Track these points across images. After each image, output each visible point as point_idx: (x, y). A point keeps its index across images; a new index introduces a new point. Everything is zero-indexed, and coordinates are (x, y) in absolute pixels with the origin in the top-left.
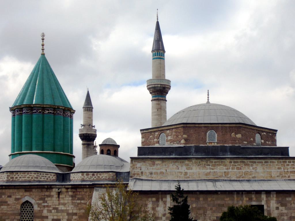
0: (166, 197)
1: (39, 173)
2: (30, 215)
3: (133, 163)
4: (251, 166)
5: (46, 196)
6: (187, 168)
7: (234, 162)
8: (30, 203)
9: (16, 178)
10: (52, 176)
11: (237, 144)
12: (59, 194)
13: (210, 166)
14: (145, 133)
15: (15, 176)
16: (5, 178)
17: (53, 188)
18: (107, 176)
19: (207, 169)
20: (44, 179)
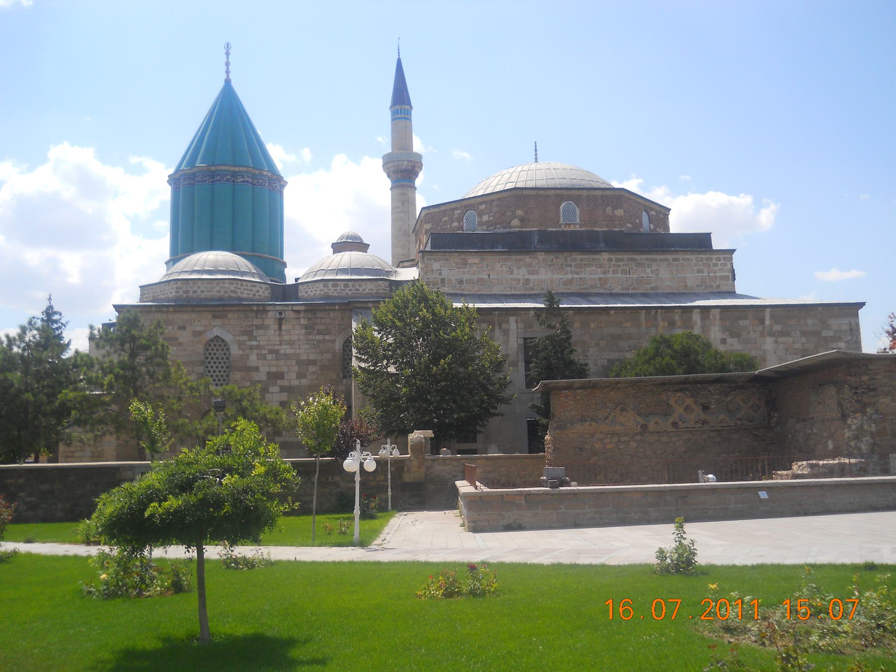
0: (507, 322)
1: (240, 283)
3: (426, 262)
4: (648, 268)
5: (254, 327)
6: (528, 271)
7: (618, 260)
8: (223, 341)
9: (195, 292)
10: (263, 290)
11: (616, 227)
12: (280, 321)
14: (433, 213)
17: (269, 311)
18: (374, 288)
19: (567, 274)
20: (247, 294)
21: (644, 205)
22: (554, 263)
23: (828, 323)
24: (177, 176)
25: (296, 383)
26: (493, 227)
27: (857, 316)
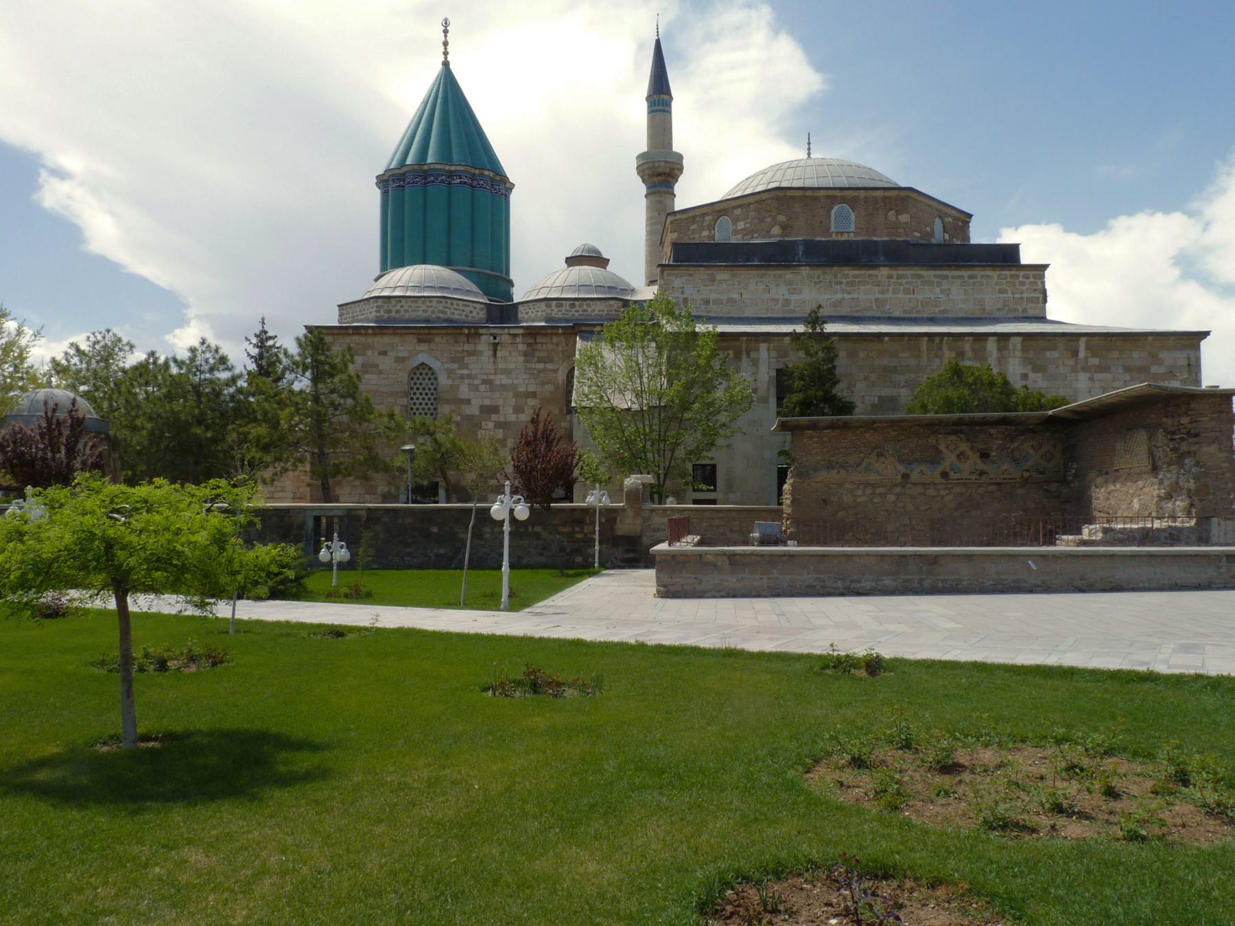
0: (758, 350)
1: (449, 301)
2: (429, 396)
3: (666, 278)
5: (465, 353)
7: (899, 277)
8: (430, 369)
9: (398, 312)
10: (478, 310)
11: (900, 237)
12: (495, 346)
13: (843, 286)
14: (680, 219)
15: (394, 306)
16: (371, 313)
17: (482, 334)
19: (836, 293)
21: (937, 209)
22: (821, 279)
23: (1159, 356)
24: (385, 178)
25: (512, 418)
26: (750, 237)
27: (1197, 348)
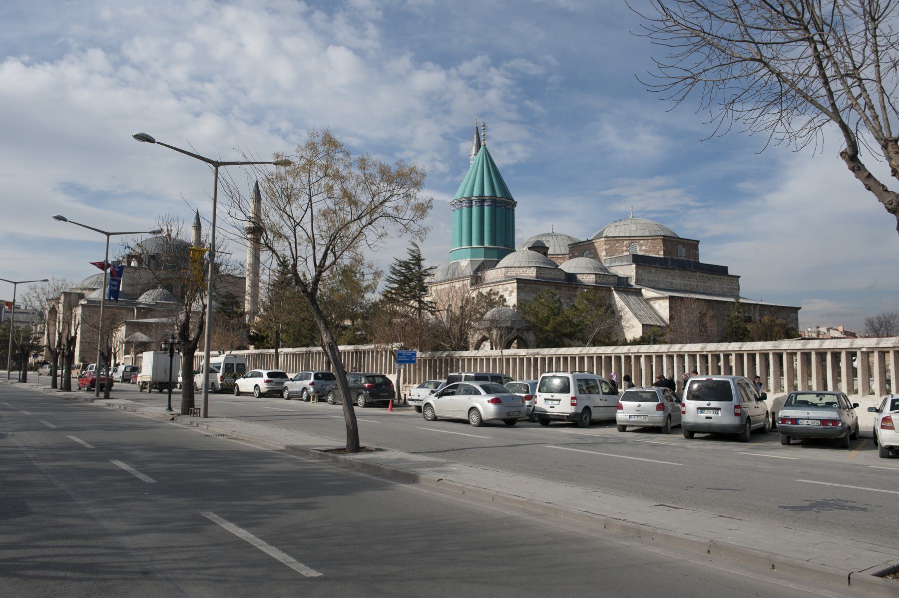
9: (544, 274)
15: (542, 272)
27: (797, 313)
